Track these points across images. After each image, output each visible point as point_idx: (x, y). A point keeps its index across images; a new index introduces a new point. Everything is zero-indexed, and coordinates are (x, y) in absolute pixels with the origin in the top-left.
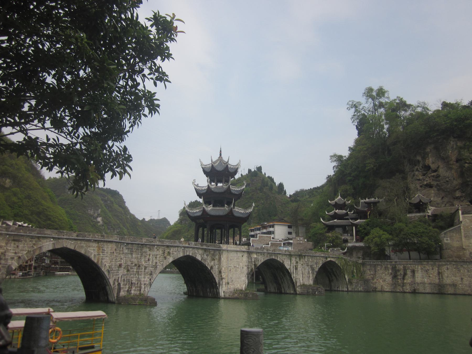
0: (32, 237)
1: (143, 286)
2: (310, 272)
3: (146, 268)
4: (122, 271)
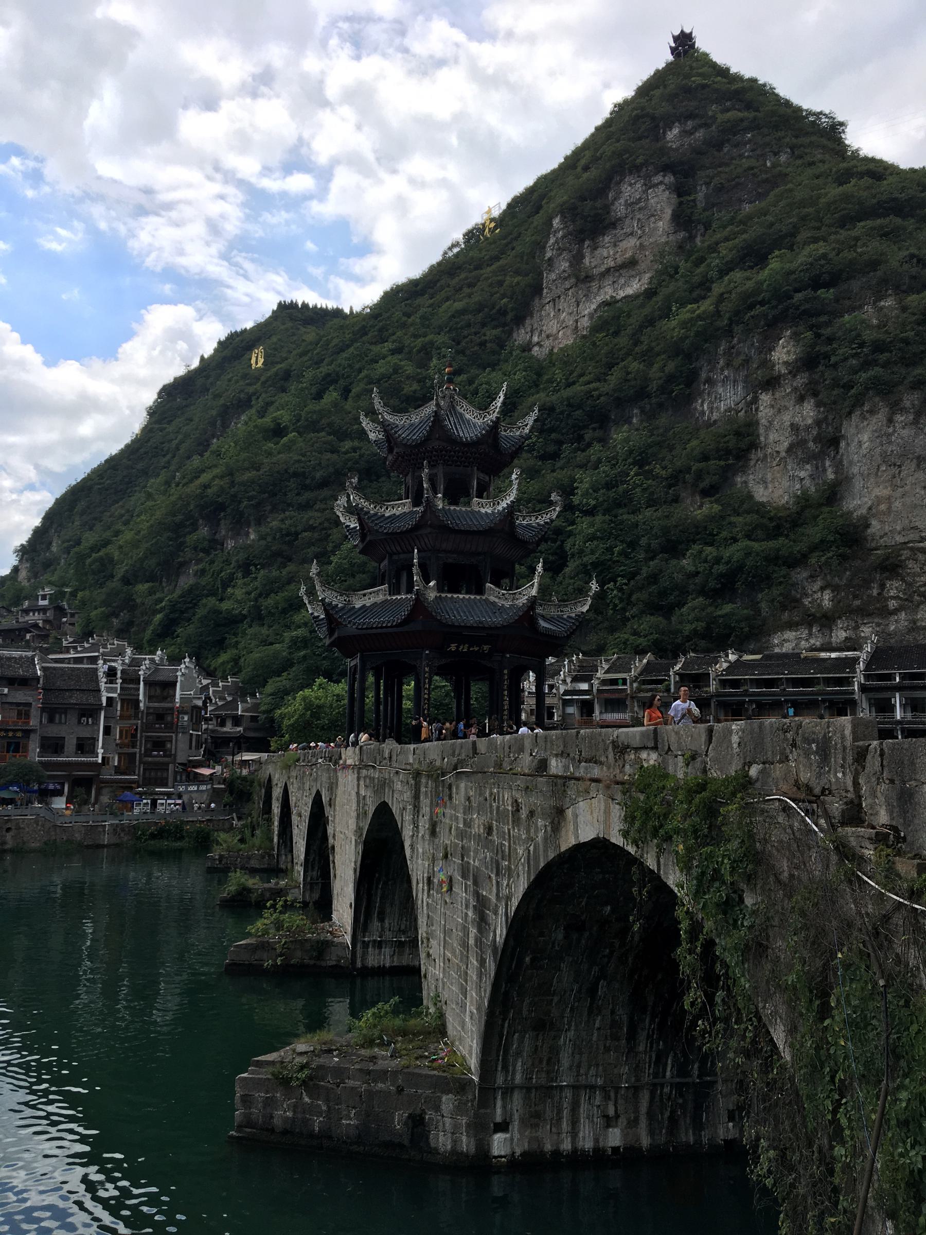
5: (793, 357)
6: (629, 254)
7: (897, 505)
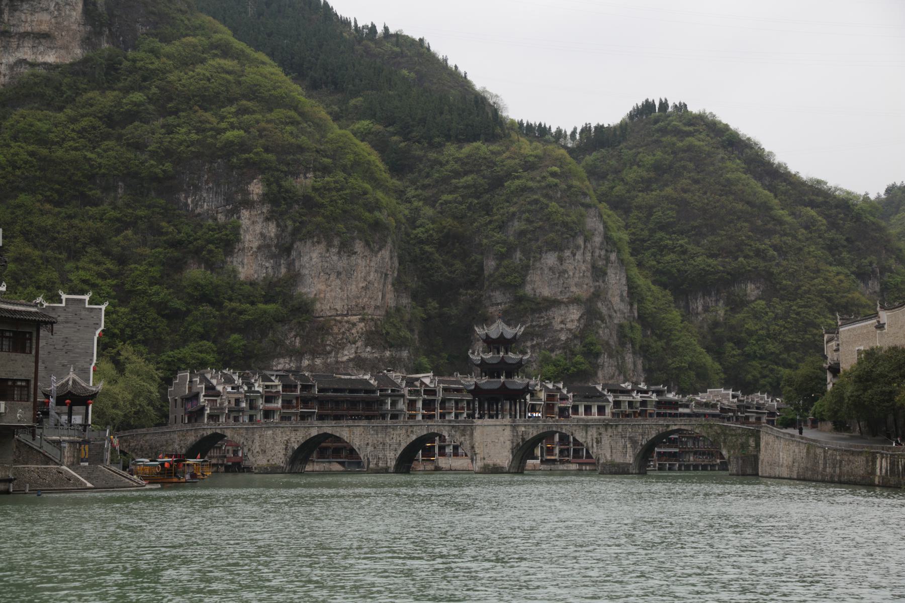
0: (305, 427)
1: (389, 460)
2: (629, 446)
3: (390, 446)
4: (370, 448)
5: (261, 192)
6: (44, 28)
7: (328, 295)
